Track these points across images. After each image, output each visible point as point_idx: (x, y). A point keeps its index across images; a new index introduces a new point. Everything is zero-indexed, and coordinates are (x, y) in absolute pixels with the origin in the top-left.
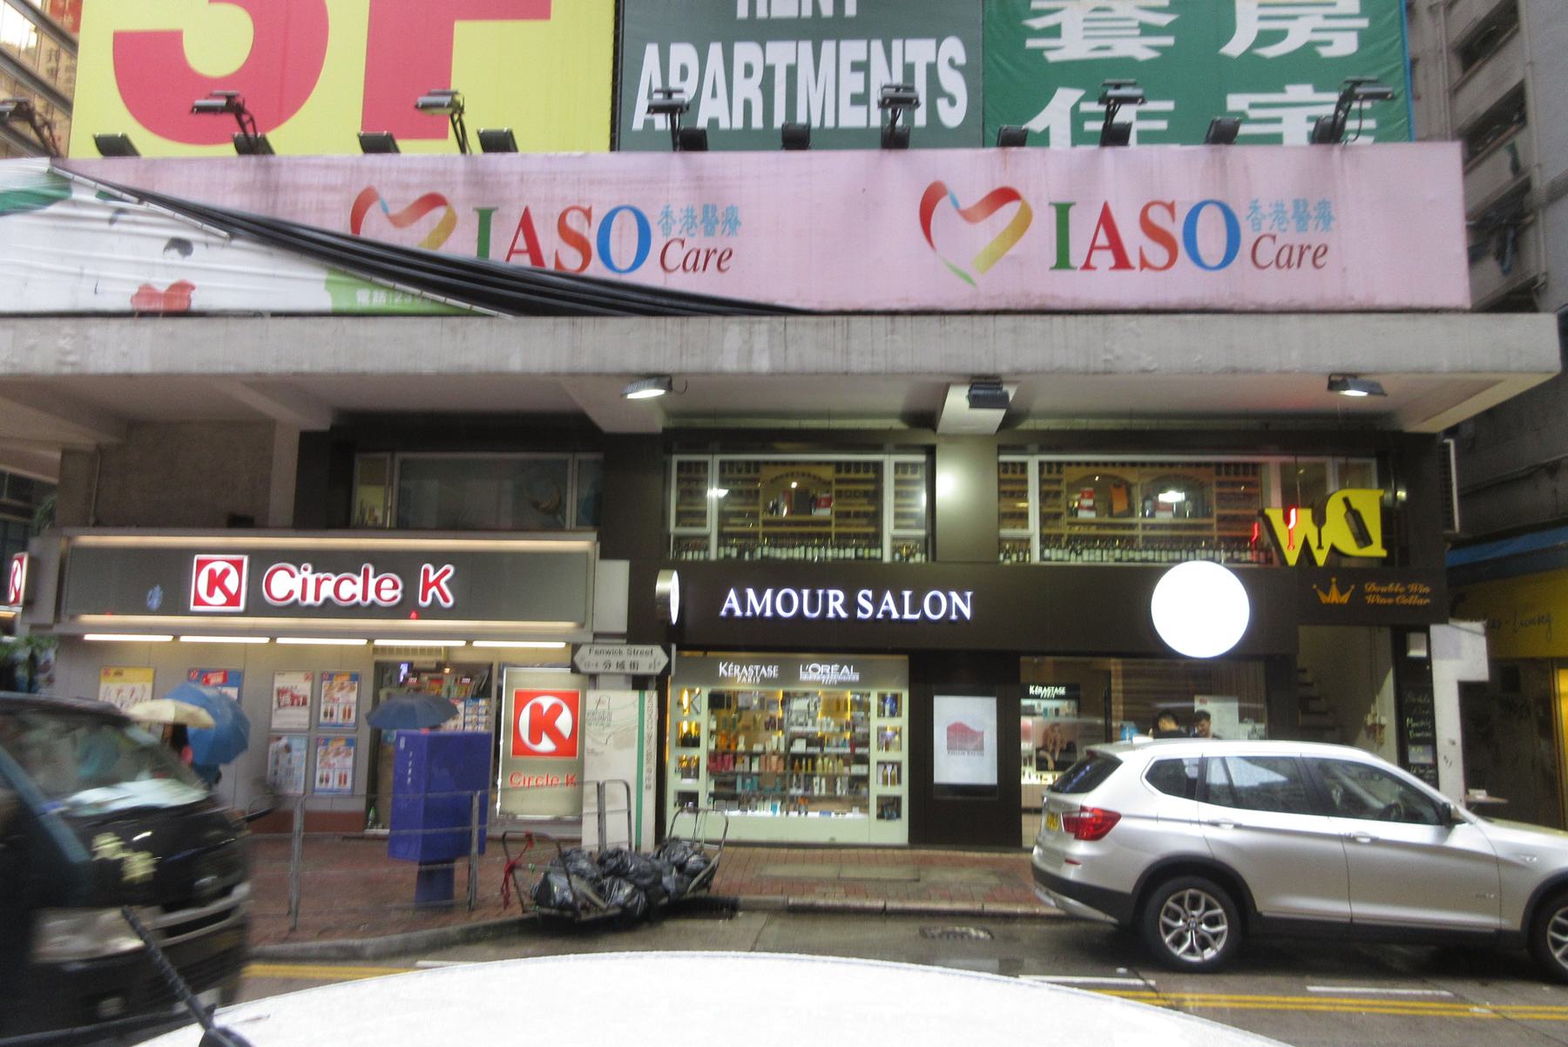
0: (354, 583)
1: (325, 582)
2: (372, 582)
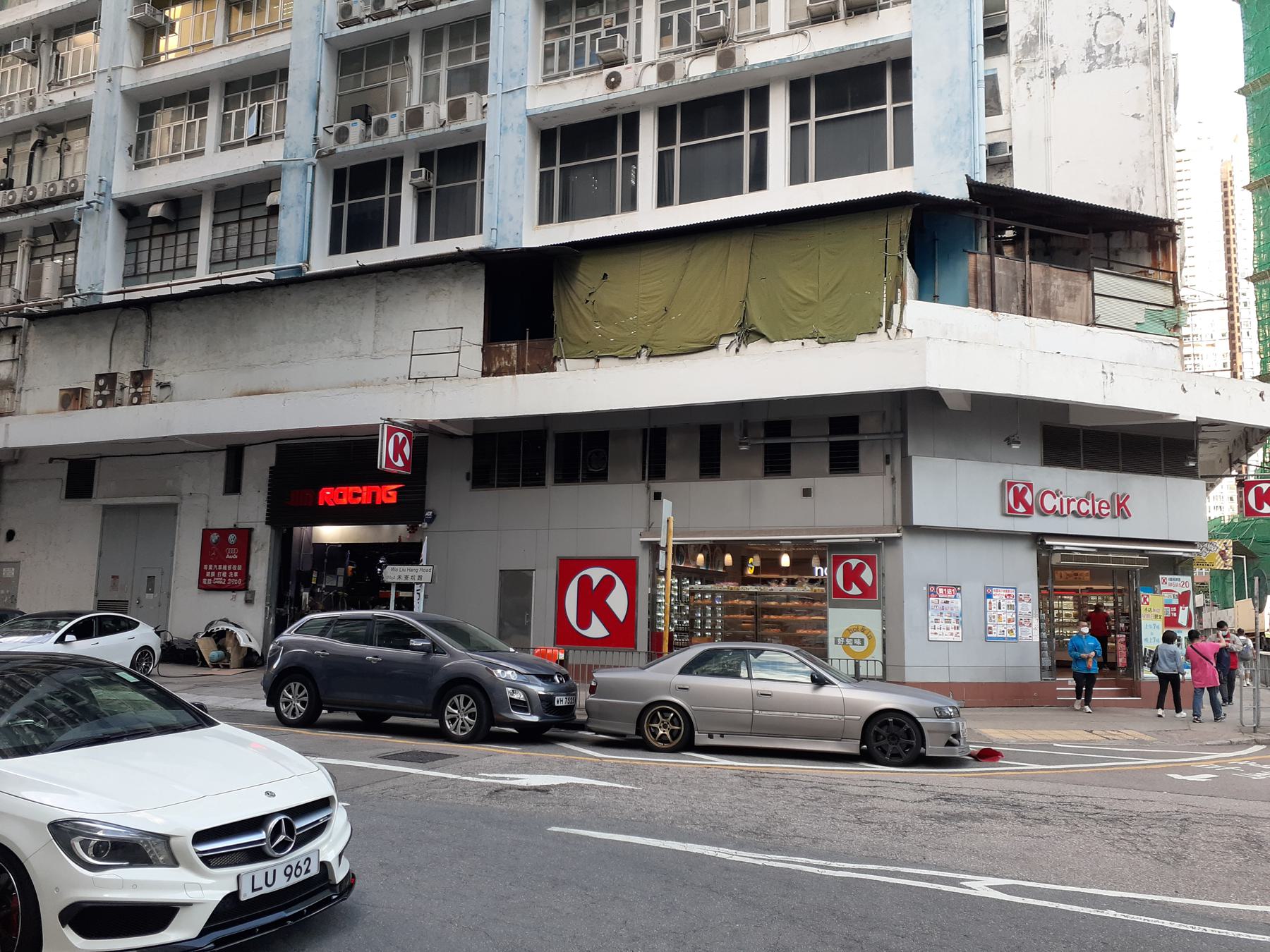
0: (1088, 504)
1: (1072, 503)
2: (1097, 504)
